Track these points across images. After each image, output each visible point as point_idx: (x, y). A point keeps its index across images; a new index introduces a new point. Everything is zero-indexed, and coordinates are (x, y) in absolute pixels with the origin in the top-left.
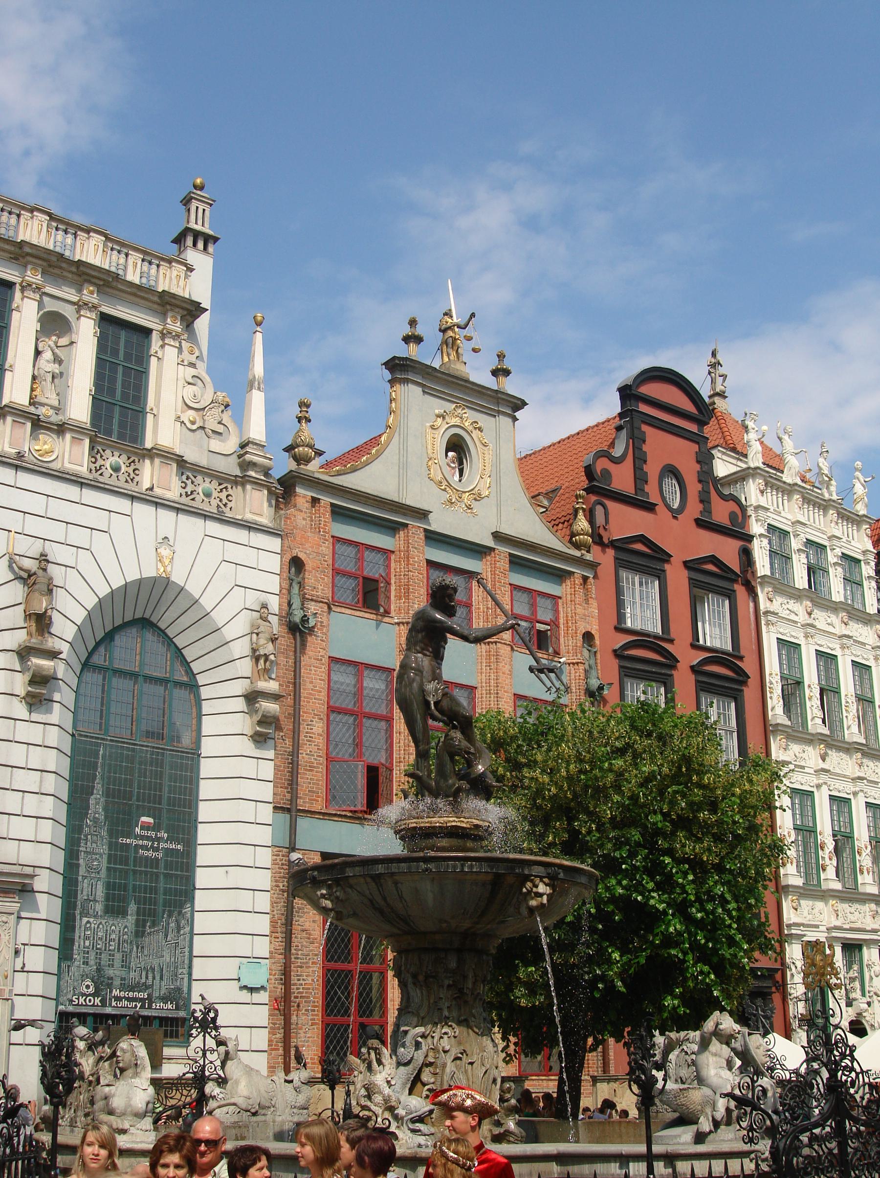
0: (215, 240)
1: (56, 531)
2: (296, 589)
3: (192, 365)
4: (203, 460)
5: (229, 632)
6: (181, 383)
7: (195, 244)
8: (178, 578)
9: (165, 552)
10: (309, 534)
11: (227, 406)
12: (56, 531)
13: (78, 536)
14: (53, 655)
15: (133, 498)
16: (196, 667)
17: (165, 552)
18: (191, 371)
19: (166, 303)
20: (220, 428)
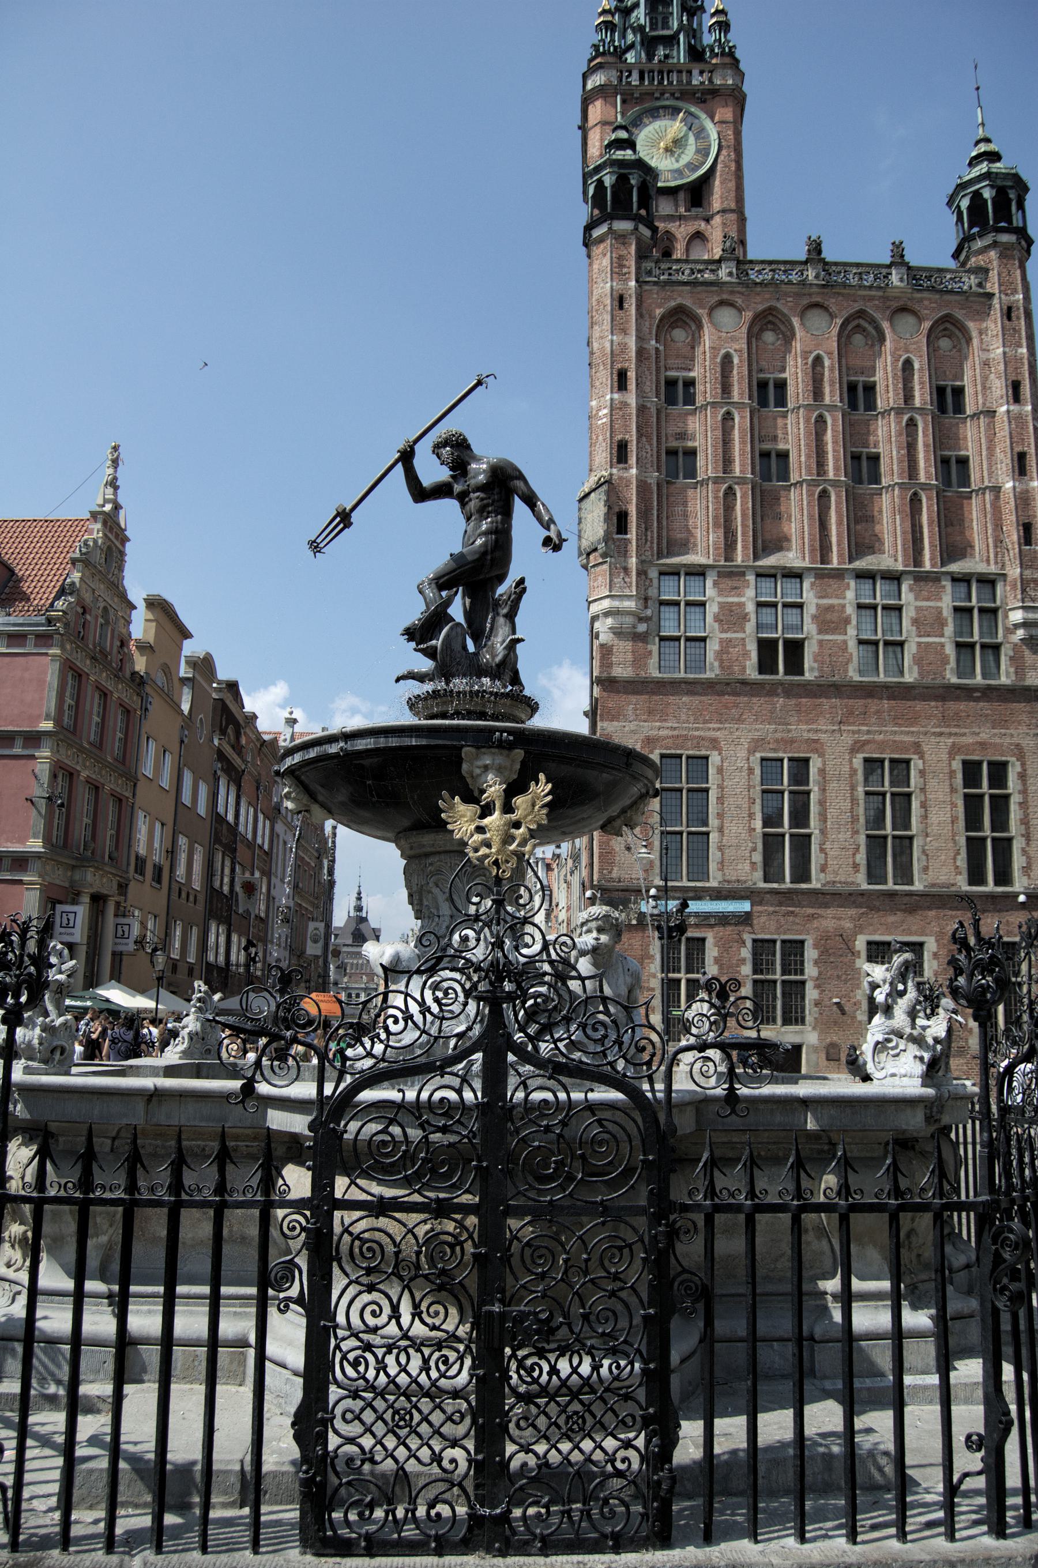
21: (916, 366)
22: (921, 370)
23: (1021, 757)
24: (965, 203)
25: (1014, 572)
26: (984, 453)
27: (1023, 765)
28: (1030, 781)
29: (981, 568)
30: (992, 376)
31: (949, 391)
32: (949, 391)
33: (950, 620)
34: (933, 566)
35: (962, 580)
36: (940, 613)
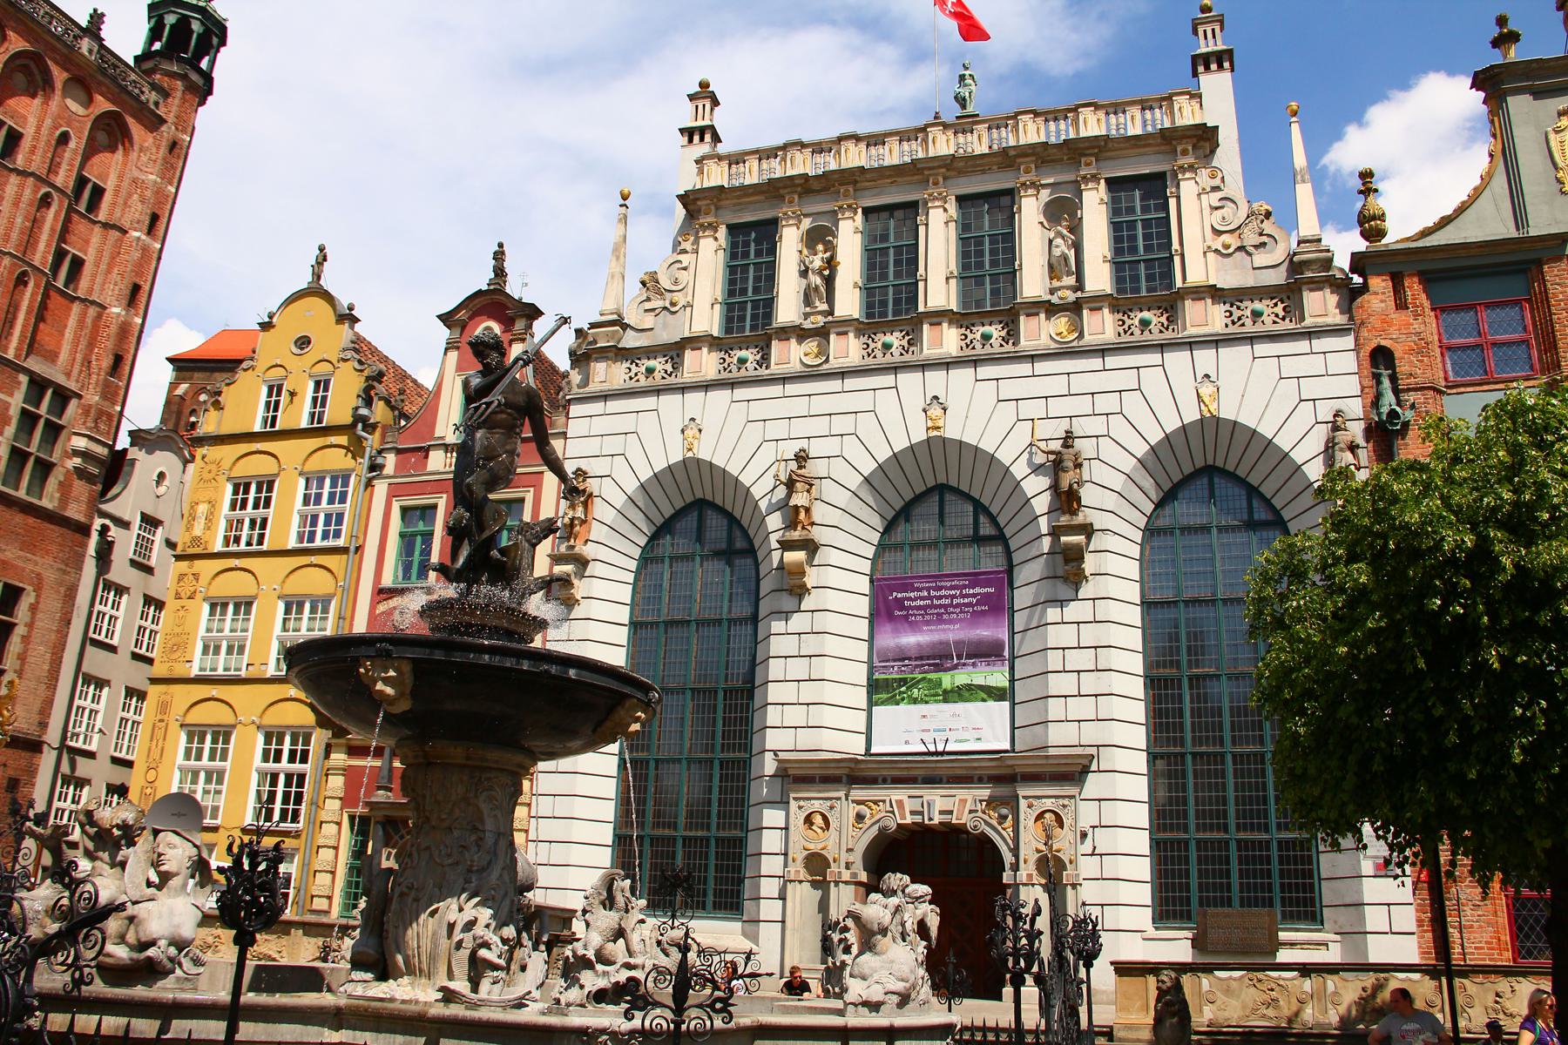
0: (1230, 53)
1: (1083, 405)
2: (1386, 383)
3: (1216, 189)
4: (1250, 283)
5: (1298, 456)
6: (1207, 211)
7: (1207, 68)
8: (1227, 413)
9: (1207, 390)
10: (1397, 317)
11: (1268, 215)
12: (1083, 405)
13: (1106, 403)
14: (1088, 530)
15: (1162, 347)
16: (1277, 502)
17: (1207, 390)
18: (1219, 195)
19: (1170, 139)
20: (1264, 239)
21: (72, 144)
22: (75, 151)
23: (38, 589)
24: (170, 19)
25: (93, 397)
26: (103, 267)
27: (38, 596)
28: (40, 615)
29: (61, 379)
30: (136, 197)
31: (89, 186)
32: (89, 186)
33: (14, 422)
34: (17, 356)
35: (39, 385)
36: (7, 409)
